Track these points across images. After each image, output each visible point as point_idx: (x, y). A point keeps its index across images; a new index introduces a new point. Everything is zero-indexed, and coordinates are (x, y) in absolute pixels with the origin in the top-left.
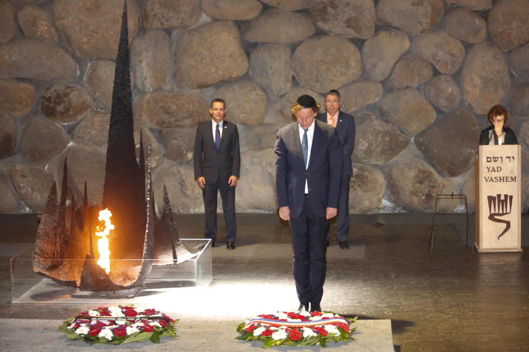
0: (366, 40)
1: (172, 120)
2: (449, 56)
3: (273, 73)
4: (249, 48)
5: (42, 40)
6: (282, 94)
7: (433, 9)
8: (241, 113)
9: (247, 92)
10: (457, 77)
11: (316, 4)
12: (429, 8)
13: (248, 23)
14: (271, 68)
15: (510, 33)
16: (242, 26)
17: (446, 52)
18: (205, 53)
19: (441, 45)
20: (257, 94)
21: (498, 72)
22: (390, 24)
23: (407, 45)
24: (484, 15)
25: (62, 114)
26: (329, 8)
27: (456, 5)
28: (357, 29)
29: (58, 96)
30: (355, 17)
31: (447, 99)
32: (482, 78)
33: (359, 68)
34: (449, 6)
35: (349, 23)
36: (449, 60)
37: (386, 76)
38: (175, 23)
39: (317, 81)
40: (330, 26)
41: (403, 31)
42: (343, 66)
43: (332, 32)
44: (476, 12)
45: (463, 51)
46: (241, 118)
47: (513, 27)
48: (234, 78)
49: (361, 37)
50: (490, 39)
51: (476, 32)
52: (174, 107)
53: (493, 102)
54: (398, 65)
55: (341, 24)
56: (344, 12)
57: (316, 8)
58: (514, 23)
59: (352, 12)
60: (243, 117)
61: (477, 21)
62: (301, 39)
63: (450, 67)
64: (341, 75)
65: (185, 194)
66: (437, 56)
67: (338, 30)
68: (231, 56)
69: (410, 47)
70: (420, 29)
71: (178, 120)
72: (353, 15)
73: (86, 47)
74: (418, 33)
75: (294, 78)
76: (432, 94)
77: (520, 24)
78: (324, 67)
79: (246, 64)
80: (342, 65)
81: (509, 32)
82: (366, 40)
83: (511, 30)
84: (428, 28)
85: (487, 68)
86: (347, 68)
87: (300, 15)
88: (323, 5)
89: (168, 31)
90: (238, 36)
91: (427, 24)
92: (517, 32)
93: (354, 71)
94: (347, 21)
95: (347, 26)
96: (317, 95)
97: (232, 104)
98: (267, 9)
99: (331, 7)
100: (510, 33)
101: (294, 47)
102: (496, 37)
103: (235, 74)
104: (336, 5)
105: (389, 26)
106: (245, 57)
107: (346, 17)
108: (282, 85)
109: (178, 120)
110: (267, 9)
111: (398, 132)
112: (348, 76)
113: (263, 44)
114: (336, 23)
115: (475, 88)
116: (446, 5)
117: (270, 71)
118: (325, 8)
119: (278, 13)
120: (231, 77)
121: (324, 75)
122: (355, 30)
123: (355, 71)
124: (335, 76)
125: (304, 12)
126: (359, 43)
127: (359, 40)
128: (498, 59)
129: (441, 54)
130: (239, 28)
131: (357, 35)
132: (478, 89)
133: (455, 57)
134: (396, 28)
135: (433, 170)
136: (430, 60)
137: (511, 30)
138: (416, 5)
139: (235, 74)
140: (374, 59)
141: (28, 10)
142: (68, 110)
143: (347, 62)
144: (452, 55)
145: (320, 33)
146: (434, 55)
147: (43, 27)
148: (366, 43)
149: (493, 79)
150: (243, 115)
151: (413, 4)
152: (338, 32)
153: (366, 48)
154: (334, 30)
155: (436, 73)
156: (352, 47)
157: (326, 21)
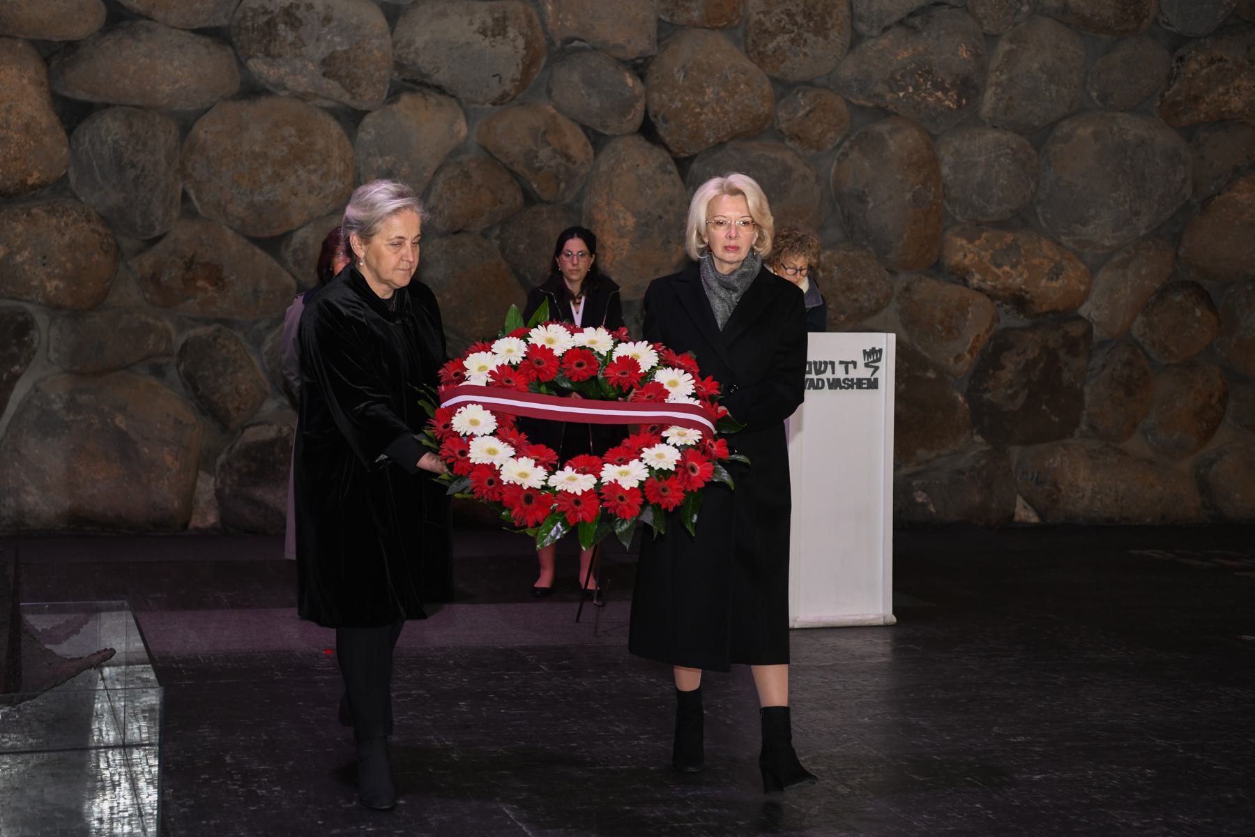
0: (367, 112)
2: (559, 159)
3: (137, 177)
4: (73, 114)
6: (156, 233)
7: (528, 46)
8: (50, 277)
9: (67, 225)
11: (250, 14)
12: (521, 43)
14: (133, 166)
15: (700, 114)
16: (55, 55)
17: (554, 150)
19: (545, 133)
20: (93, 231)
21: (671, 203)
22: (427, 76)
23: (462, 128)
24: (640, 68)
27: (576, 43)
28: (351, 84)
30: (346, 52)
34: (559, 44)
35: (329, 66)
36: (562, 169)
40: (282, 71)
41: (452, 96)
42: (315, 171)
43: (285, 89)
44: (622, 62)
45: (590, 149)
46: (49, 289)
47: (706, 99)
48: (33, 187)
49: (355, 104)
50: (648, 130)
53: (657, 271)
54: (442, 175)
55: (311, 66)
56: (318, 40)
57: (249, 24)
58: (709, 91)
59: (337, 39)
60: (57, 288)
61: (630, 81)
63: (562, 185)
64: (310, 192)
66: (537, 157)
67: (302, 83)
68: (27, 128)
69: (467, 137)
70: (496, 93)
72: (339, 48)
74: (488, 106)
76: (522, 247)
77: (722, 94)
78: (269, 170)
79: (65, 150)
80: (312, 167)
81: (698, 110)
82: (367, 112)
83: (702, 106)
84: (512, 93)
85: (649, 192)
86: (325, 176)
88: (266, 18)
90: (45, 80)
91: (513, 80)
92: (714, 112)
94: (324, 62)
95: (324, 75)
96: (245, 241)
97: (26, 254)
98: (118, 18)
99: (286, 24)
100: (700, 114)
102: (665, 120)
103: (36, 175)
104: (301, 21)
105: (421, 84)
107: (322, 51)
110: (118, 18)
112: (326, 197)
113: (108, 106)
114: (299, 64)
115: (621, 237)
116: (551, 42)
118: (271, 24)
119: (149, 30)
120: (23, 183)
121: (267, 188)
122: (344, 86)
123: (341, 186)
124: (296, 195)
125: (216, 35)
126: (351, 118)
127: (354, 111)
128: (671, 173)
129: (544, 153)
130: (46, 61)
131: (347, 98)
132: (626, 240)
133: (575, 163)
134: (440, 90)
136: (518, 168)
137: (702, 106)
138: (489, 33)
139: (36, 175)
140: (387, 158)
143: (324, 161)
144: (568, 157)
145: (252, 90)
148: (367, 120)
149: (660, 217)
150: (55, 283)
151: (484, 32)
152: (301, 90)
153: (368, 131)
154: (290, 84)
155: (530, 198)
156: (335, 128)
157: (273, 57)
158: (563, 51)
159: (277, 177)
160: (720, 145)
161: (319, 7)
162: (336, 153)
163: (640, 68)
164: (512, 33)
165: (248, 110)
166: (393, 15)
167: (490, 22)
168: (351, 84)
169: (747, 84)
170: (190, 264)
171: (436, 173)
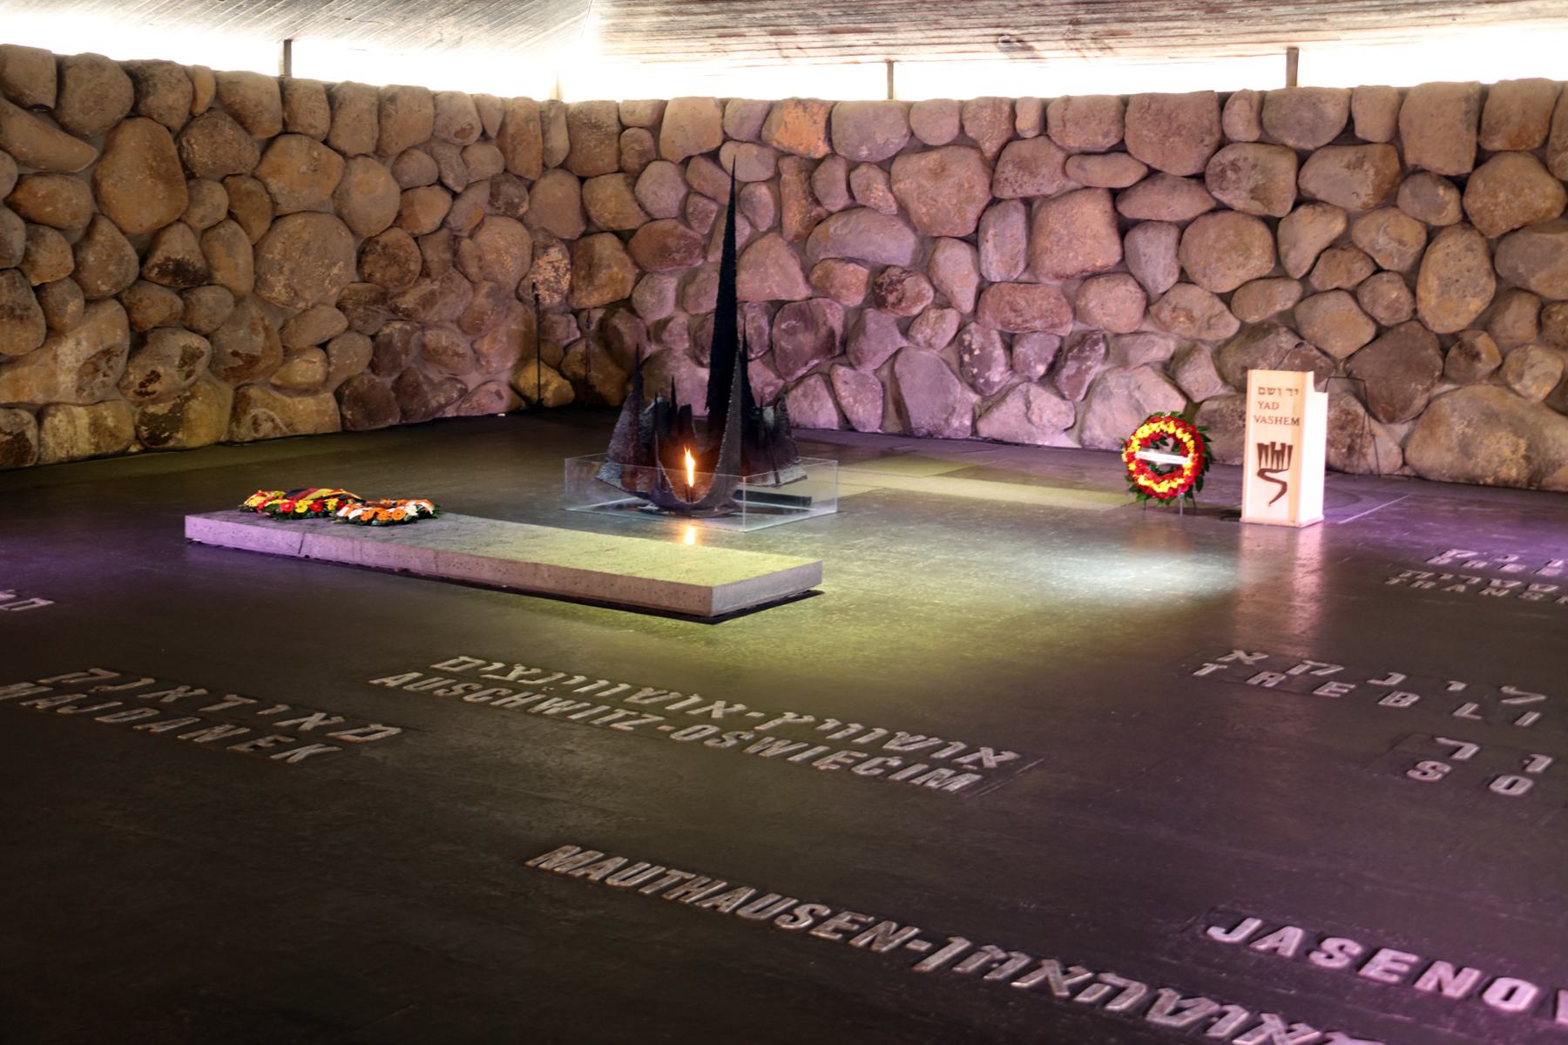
1: (1019, 320)
4: (1124, 228)
5: (876, 210)
6: (1161, 290)
7: (1376, 174)
10: (1411, 279)
12: (1372, 172)
13: (1124, 190)
18: (1062, 231)
23: (1338, 226)
24: (1460, 183)
25: (894, 305)
26: (1229, 173)
28: (1266, 201)
29: (891, 283)
31: (1387, 308)
32: (1440, 278)
33: (1267, 257)
35: (1255, 193)
37: (1305, 271)
38: (1030, 191)
39: (1205, 275)
51: (1440, 208)
52: (1023, 303)
62: (1189, 215)
65: (1029, 421)
67: (1239, 204)
71: (1026, 321)
73: (925, 220)
75: (1182, 271)
86: (1247, 258)
87: (1193, 181)
89: (1028, 202)
93: (1260, 262)
94: (1252, 191)
98: (1152, 174)
101: (1183, 227)
106: (1115, 239)
107: (1251, 184)
108: (1160, 279)
109: (1026, 321)
111: (1316, 352)
117: (1143, 259)
118: (1223, 171)
126: (1272, 223)
131: (1266, 212)
135: (1361, 411)
136: (1367, 250)
141: (863, 169)
142: (900, 301)
144: (1401, 242)
145: (1220, 208)
146: (1373, 242)
147: (878, 193)
151: (1348, 167)
153: (1283, 229)
155: (1379, 270)
156: (1260, 229)
158: (1408, 172)
159: (1219, 259)
160: (1514, 231)
161: (1251, 159)
162: (1257, 244)
163: (1460, 183)
164: (1366, 166)
165: (1211, 220)
166: (1302, 158)
167: (1353, 159)
168: (1266, 201)
169: (1531, 188)
170: (1174, 309)
171: (1317, 259)
